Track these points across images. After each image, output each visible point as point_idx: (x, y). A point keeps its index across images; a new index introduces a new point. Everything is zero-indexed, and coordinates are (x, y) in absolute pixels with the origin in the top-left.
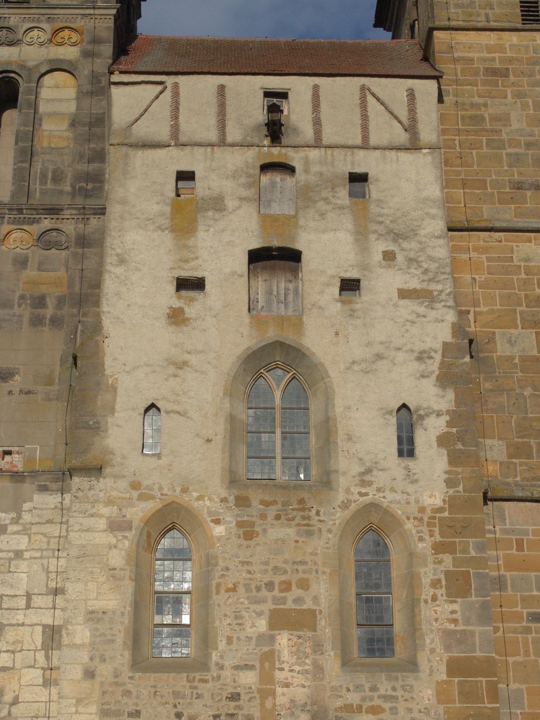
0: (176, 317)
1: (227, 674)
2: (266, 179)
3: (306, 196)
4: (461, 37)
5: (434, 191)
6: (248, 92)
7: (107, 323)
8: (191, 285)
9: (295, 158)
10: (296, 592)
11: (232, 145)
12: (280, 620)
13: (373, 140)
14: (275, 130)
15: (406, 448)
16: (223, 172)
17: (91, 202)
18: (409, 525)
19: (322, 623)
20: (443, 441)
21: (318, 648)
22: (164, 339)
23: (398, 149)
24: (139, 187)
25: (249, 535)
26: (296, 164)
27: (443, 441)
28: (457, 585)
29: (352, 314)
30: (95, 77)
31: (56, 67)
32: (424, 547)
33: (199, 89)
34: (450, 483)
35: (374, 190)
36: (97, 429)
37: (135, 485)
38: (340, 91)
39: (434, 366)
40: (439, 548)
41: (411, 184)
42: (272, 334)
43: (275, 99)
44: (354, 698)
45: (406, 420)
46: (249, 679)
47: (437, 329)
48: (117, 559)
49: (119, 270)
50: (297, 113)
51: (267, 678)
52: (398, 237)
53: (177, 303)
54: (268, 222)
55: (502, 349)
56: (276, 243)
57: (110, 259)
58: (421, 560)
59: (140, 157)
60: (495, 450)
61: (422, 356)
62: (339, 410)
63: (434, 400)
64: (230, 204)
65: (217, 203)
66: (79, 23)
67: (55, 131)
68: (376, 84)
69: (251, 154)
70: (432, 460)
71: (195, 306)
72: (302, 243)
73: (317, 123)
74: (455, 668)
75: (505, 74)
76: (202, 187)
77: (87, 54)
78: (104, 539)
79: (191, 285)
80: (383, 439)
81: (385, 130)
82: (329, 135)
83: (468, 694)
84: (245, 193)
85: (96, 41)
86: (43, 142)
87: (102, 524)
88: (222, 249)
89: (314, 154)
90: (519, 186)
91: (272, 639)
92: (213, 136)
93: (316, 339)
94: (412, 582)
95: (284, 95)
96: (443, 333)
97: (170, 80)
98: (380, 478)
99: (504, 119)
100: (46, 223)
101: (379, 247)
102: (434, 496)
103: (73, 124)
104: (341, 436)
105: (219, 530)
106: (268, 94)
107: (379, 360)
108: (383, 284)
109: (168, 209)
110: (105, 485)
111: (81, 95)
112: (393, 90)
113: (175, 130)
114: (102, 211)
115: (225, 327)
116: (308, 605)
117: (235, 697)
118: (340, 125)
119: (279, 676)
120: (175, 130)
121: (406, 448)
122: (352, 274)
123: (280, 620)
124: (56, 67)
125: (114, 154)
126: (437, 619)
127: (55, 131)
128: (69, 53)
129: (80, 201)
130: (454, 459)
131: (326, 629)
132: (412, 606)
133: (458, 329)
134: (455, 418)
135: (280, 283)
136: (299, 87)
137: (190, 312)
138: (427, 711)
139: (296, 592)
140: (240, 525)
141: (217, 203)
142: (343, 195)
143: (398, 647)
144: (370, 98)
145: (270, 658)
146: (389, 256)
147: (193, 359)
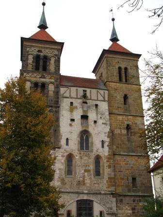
0: (71, 125)
1: (78, 178)
2: (83, 104)
3: (89, 107)
4: (111, 83)
5: (107, 108)
6: (81, 90)
7: (61, 125)
8: (73, 120)
9: (88, 101)
10: (88, 167)
11: (79, 98)
12: (86, 171)
13: (99, 99)
14: (85, 96)
15: (103, 147)
16: (77, 103)
17: (57, 105)
18: (103, 158)
19: (91, 171)
20: (108, 146)
21: (91, 175)
22: (69, 128)
23: (102, 101)
24: (65, 104)
25: (81, 158)
26: (88, 102)
27: (108, 146)
28: (109, 167)
29: (96, 126)
30: (57, 85)
31: (51, 83)
32: (105, 161)
33: (73, 89)
34: (109, 152)
35: (98, 107)
36: (60, 141)
37: (65, 150)
38: (94, 91)
39: (107, 135)
40: (107, 161)
41: (104, 106)
42: (84, 129)
43: (85, 91)
44: (96, 182)
45: (103, 142)
46: (81, 179)
47: (107, 129)
48: (63, 161)
49: (62, 117)
50: (88, 94)
51: (84, 179)
52: (102, 115)
53: (71, 123)
54: (84, 111)
55: (116, 132)
56: (85, 114)
57: (61, 115)
58: (104, 163)
59: (65, 99)
60: (115, 147)
61: (105, 133)
62: (94, 140)
63: (107, 140)
64: (78, 108)
65: (76, 107)
66: (55, 76)
67: (51, 93)
68: (100, 91)
69: (81, 100)
70: (106, 149)
71: (73, 124)
72: (88, 115)
73: (91, 96)
74: (109, 178)
75: (117, 89)
76: (74, 105)
77: (56, 81)
78: (61, 158)
79: (73, 120)
80: (99, 145)
81: (101, 98)
82: (92, 99)
83: (111, 182)
84: (80, 106)
85: (57, 79)
86: (49, 95)
87: (60, 156)
88: (77, 114)
89: (90, 101)
90: (119, 107)
91: (84, 173)
92: (75, 97)
93: (90, 130)
94: (104, 167)
95: (86, 91)
96: (108, 130)
97: (69, 87)
98: (99, 151)
99: (116, 97)
100: (50, 108)
101: (100, 116)
102: (107, 154)
103: (54, 92)
104: (94, 145)
105: (77, 157)
106: (84, 91)
107: (100, 133)
108: (100, 122)
109: (69, 108)
110: (61, 150)
111: (55, 88)
112: (102, 92)
113: (70, 95)
114: (59, 107)
115: (77, 127)
116: (89, 169)
117: (79, 181)
118: (94, 97)
119: (86, 179)
120: (70, 95)
121: (103, 147)
122: (96, 120)
123: (86, 171)
124: (51, 83)
125: (60, 99)
126: (106, 172)
127: (51, 93)
128: (53, 80)
129: (55, 105)
130: (109, 148)
131: (92, 172)
132: (103, 170)
133: (110, 129)
134: (110, 142)
135: (85, 121)
136: (88, 90)
137: (73, 124)
138: (105, 184)
139: (88, 167)
140: (80, 157)
141: (76, 107)
142: (94, 108)
143: (101, 175)
144: (99, 94)
145: (84, 176)
146: (101, 118)
147: (73, 132)
